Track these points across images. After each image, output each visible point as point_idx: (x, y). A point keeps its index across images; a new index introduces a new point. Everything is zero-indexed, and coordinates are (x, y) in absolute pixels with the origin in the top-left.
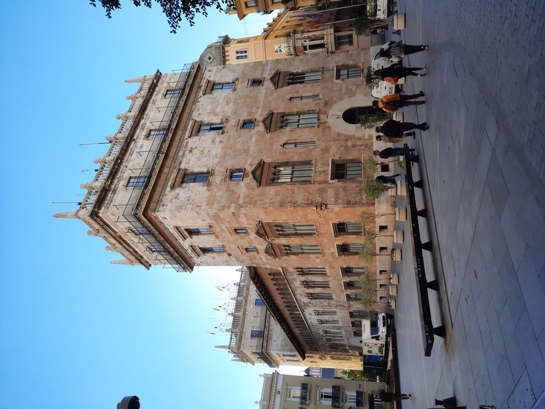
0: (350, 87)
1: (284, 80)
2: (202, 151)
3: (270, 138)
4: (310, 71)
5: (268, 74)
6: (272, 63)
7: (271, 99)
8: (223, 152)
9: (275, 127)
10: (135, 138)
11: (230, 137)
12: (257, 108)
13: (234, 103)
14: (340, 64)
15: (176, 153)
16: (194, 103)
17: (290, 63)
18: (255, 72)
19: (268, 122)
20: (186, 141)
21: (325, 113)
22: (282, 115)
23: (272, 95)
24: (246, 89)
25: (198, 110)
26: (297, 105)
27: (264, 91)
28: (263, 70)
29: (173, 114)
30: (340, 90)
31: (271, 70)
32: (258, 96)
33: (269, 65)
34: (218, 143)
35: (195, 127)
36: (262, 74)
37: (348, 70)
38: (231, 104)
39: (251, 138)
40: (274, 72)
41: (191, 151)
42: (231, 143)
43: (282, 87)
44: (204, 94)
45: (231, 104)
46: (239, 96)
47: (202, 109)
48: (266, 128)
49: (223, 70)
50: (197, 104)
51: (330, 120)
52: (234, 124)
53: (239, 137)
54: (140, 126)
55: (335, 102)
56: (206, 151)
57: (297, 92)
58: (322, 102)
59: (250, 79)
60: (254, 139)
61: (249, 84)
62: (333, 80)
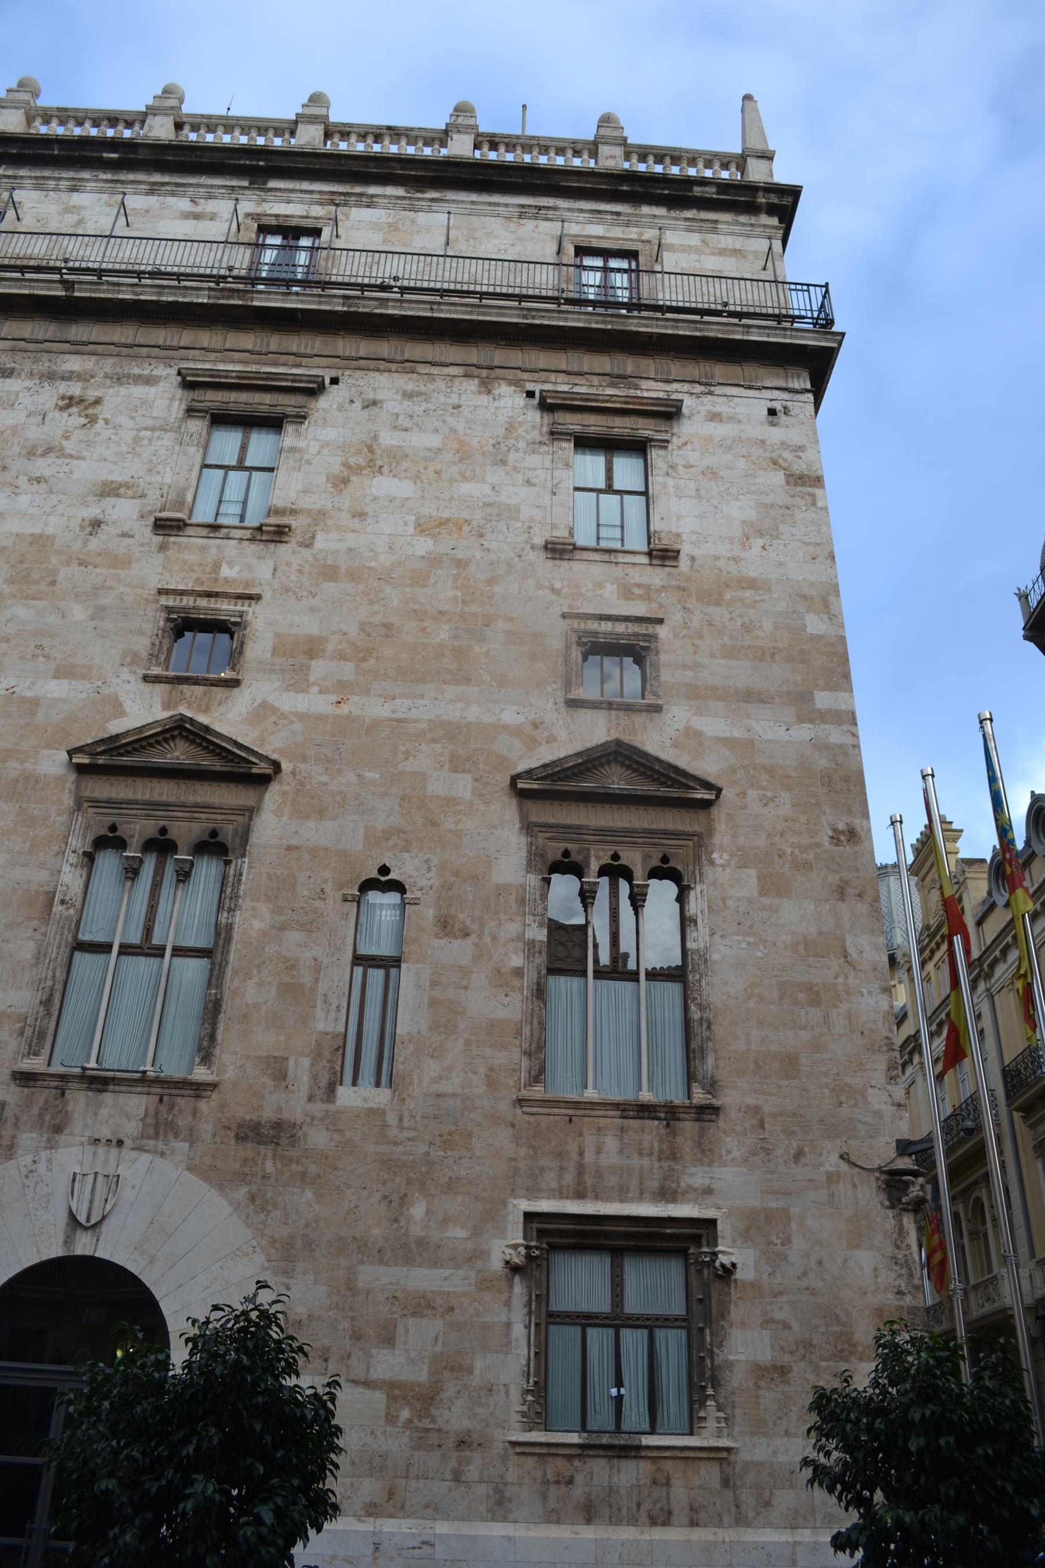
0: (420, 1334)
1: (605, 834)
2: (49, 450)
3: (31, 781)
4: (696, 1014)
5: (691, 733)
6: (821, 746)
7: (411, 766)
8: (9, 542)
9: (110, 803)
10: (272, 184)
11: (126, 562)
12: (343, 689)
13: (434, 561)
14: (729, 1250)
15: (79, 347)
16: (470, 370)
17: (806, 866)
18: (729, 653)
19: (179, 754)
20: (161, 371)
21: (159, 1128)
22: (228, 833)
23: (456, 765)
24: (557, 611)
25: (408, 396)
26: (304, 927)
27: (509, 716)
28: (749, 696)
29: (383, 288)
30: (408, 1251)
31: (744, 746)
32: (467, 680)
33: (804, 732)
34: (93, 511)
35: (257, 397)
36: (698, 695)
37: (667, 1322)
38: (423, 546)
39: (64, 672)
40: (707, 767)
41: (69, 402)
42: (63, 574)
43: (529, 828)
44: (546, 407)
45: (423, 546)
46: (492, 581)
47: (418, 407)
48: (113, 744)
49: (778, 478)
50: (472, 385)
51: (71, 1156)
52: (226, 572)
53: (99, 613)
54: (358, 189)
55: (258, 1203)
56: (43, 466)
57: (446, 926)
58: (294, 1103)
59: (662, 632)
60: (56, 689)
61: (593, 625)
62: (532, 1193)
